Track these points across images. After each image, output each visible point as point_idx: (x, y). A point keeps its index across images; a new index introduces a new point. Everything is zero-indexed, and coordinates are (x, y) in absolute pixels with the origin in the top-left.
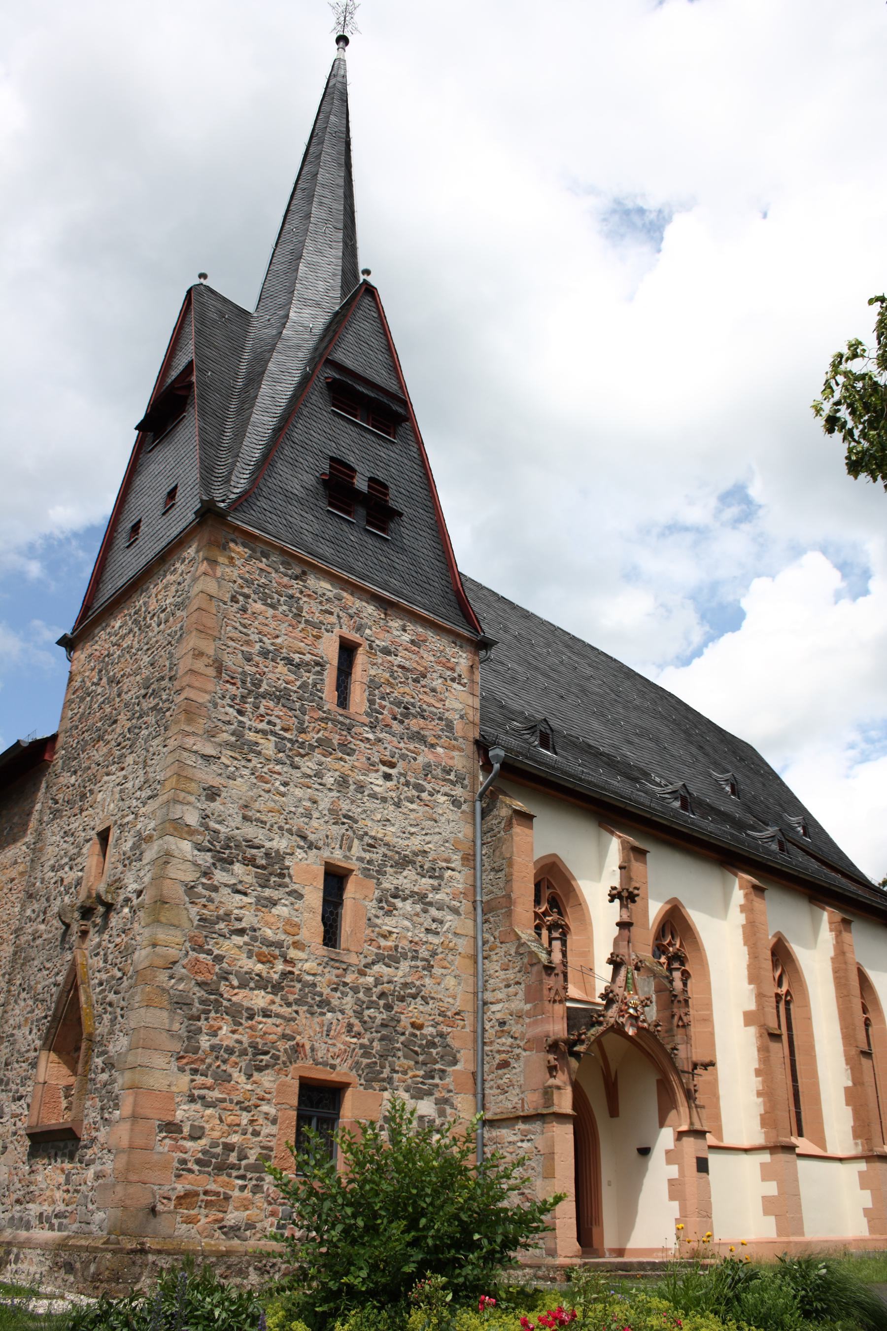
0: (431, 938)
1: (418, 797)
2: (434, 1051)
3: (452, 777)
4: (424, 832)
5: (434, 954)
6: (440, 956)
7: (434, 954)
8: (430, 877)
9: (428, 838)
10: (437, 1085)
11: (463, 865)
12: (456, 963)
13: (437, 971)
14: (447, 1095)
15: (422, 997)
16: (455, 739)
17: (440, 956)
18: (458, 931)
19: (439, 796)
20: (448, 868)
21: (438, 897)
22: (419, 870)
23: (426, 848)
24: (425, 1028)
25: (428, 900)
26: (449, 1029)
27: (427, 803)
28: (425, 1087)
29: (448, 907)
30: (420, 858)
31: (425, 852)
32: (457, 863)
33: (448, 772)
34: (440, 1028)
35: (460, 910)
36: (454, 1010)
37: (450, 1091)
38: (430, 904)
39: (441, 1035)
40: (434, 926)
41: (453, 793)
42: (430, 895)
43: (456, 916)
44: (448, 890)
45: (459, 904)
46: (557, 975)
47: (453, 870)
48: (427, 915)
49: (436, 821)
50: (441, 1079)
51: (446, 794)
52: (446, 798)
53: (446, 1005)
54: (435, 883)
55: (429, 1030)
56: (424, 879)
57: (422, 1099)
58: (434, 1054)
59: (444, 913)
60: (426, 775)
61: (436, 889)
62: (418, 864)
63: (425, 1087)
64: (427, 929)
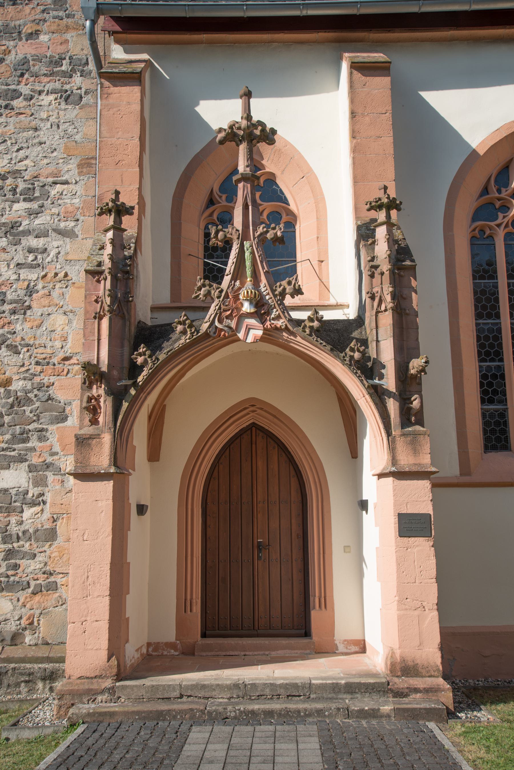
0: (24, 273)
1: (6, 107)
2: (28, 409)
3: (65, 67)
4: (16, 147)
5: (30, 291)
6: (41, 293)
7: (30, 291)
8: (25, 200)
9: (22, 154)
10: (33, 449)
11: (80, 173)
12: (67, 296)
13: (37, 310)
14: (49, 460)
15: (7, 346)
16: (68, 16)
17: (41, 293)
18: (69, 257)
19: (43, 96)
20: (55, 183)
21: (37, 222)
22: (10, 196)
23: (20, 166)
24: (13, 384)
25: (21, 229)
26: (53, 379)
27: (22, 111)
28: (13, 453)
29: (54, 230)
30: (9, 181)
31: (19, 171)
32: (70, 173)
33: (58, 63)
34: (37, 379)
35: (76, 230)
36: (61, 355)
37: (53, 454)
38: (27, 233)
39: (40, 387)
40: (31, 257)
41: (67, 87)
42: (25, 223)
43: (68, 240)
44: (55, 210)
45: (73, 224)
46: (105, 279)
47: (66, 183)
48: (19, 248)
49: (36, 129)
50: (40, 439)
51: (54, 91)
52: (52, 97)
53: (49, 350)
54: (34, 205)
55: (17, 385)
56: (16, 206)
57: (8, 467)
58: (28, 413)
59: (49, 239)
60: (22, 75)
61: (33, 214)
62: (7, 189)
63: (13, 453)
64: (18, 264)
